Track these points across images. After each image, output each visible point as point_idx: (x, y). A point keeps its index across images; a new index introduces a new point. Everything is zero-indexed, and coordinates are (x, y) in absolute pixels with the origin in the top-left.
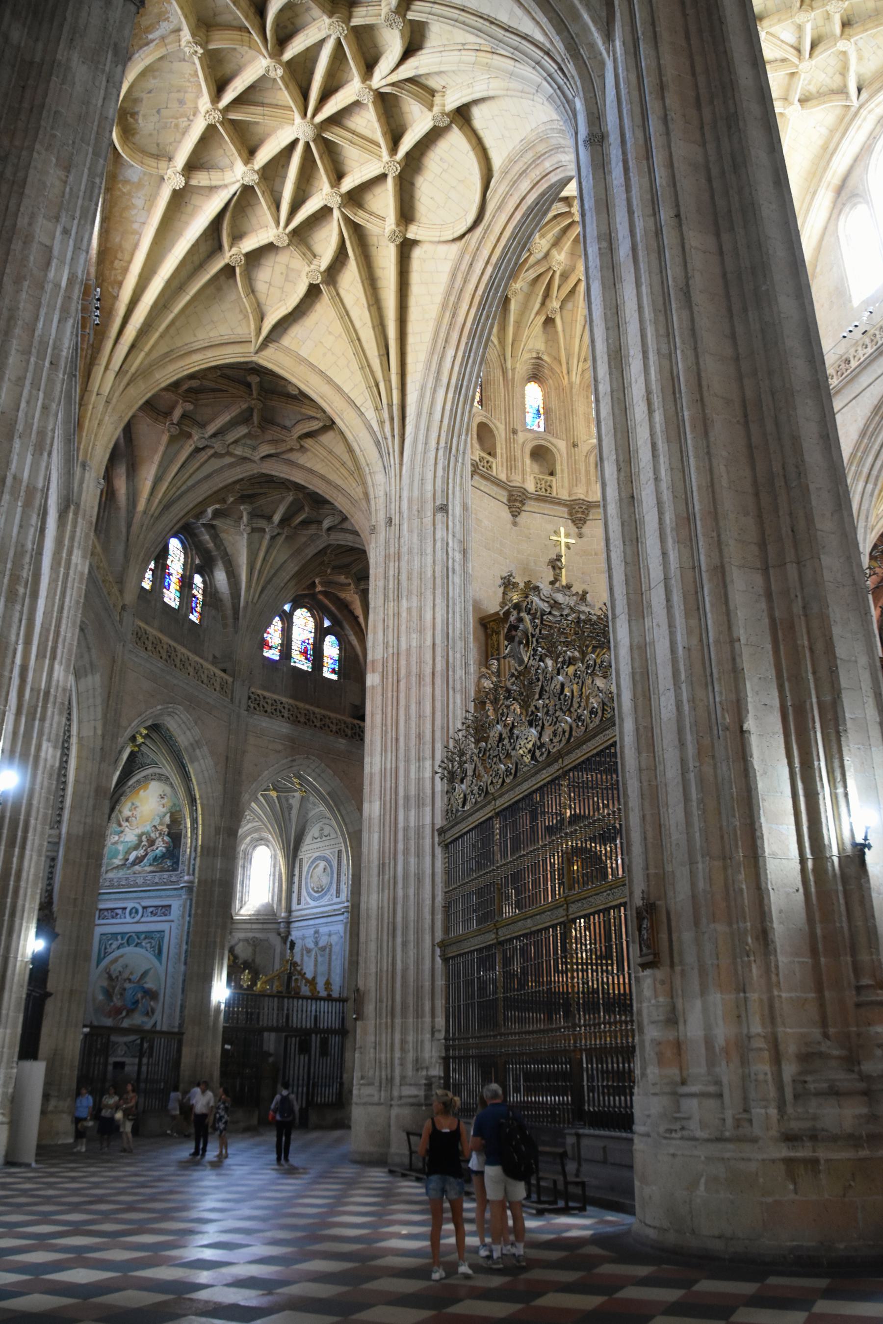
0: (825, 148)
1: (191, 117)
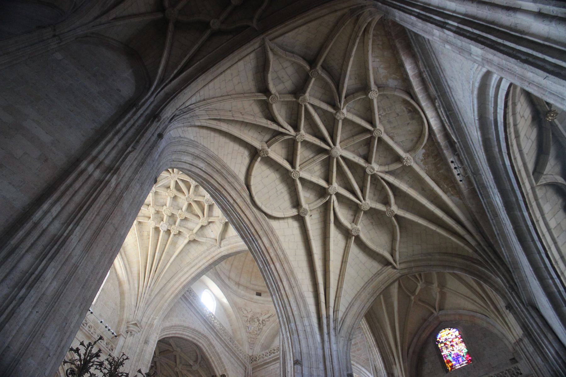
1: (380, 116)
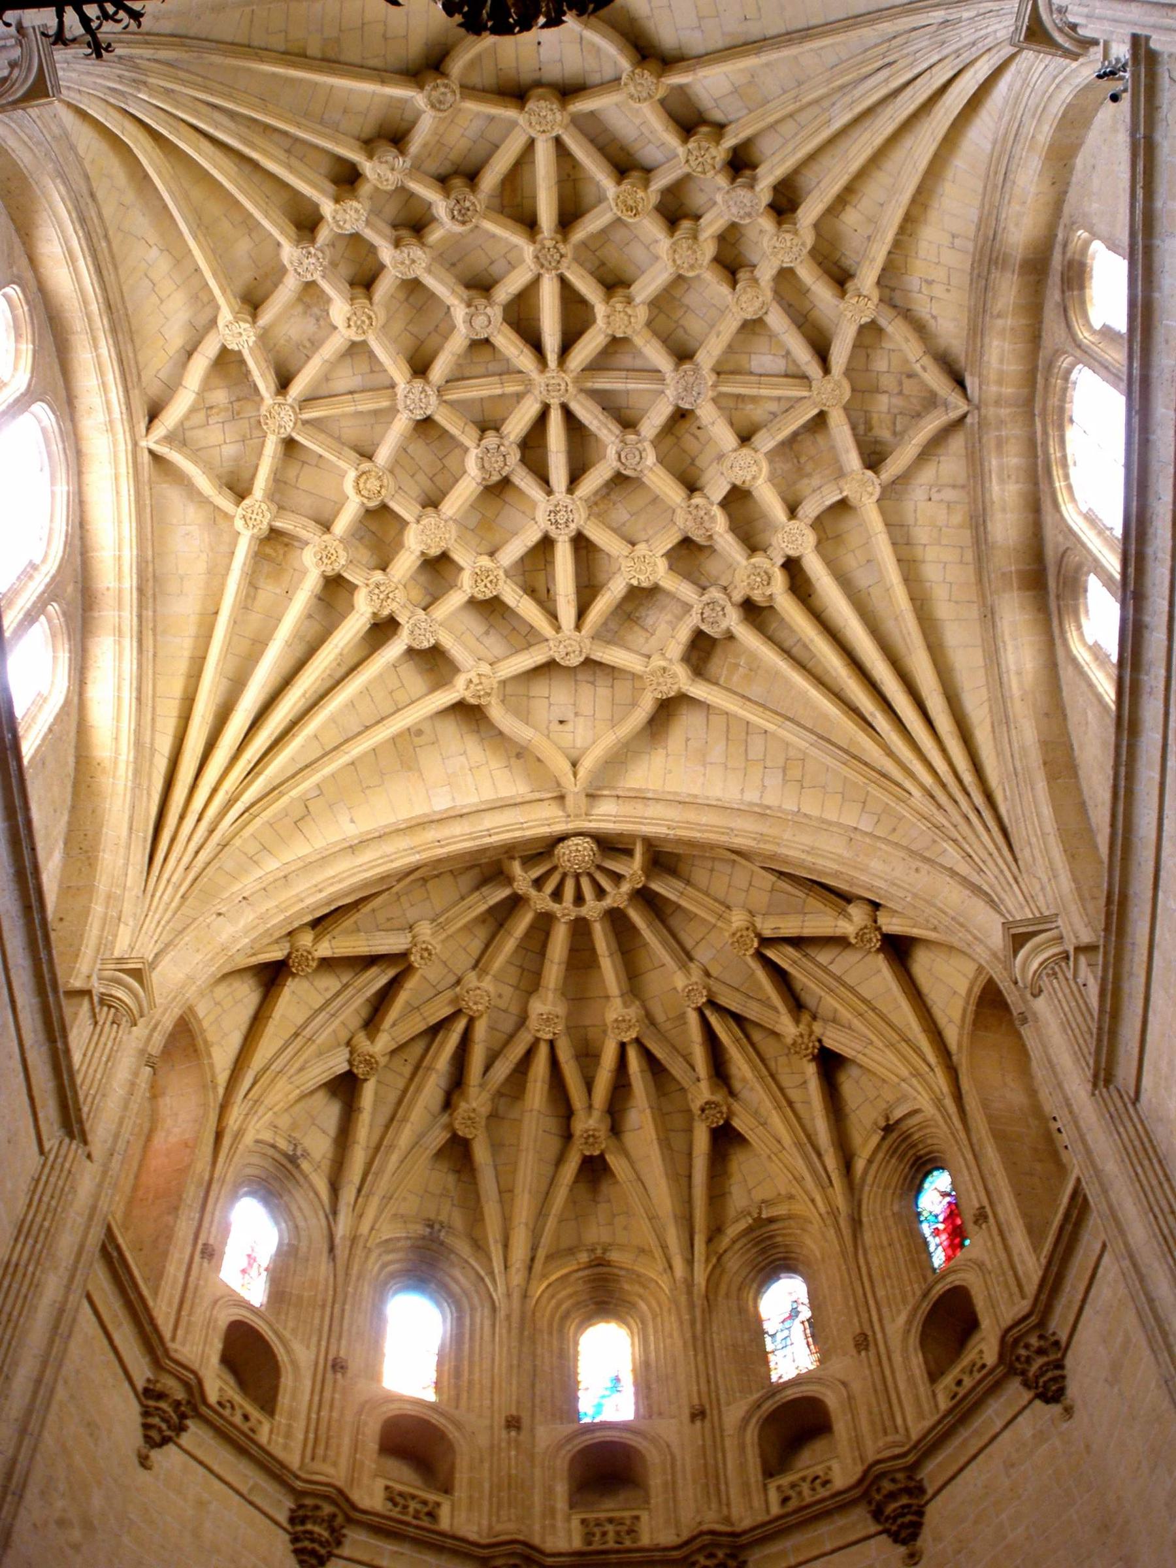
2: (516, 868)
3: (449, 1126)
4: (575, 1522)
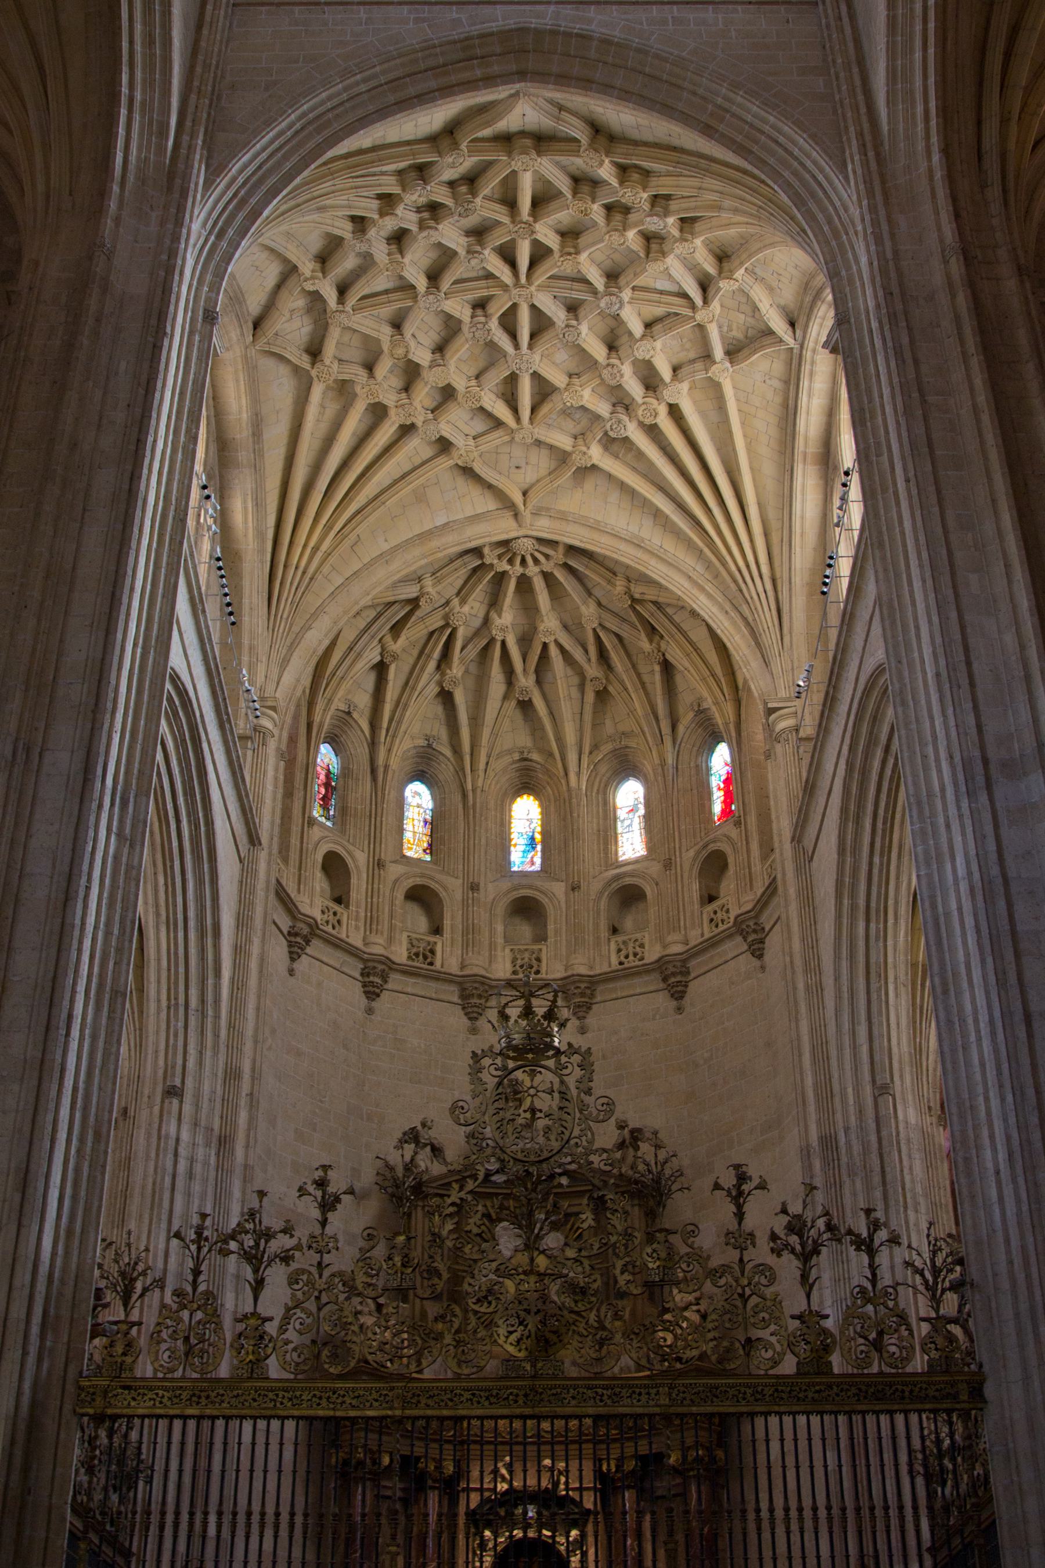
0: (785, 405)
2: (486, 551)
3: (440, 684)
4: (507, 950)
